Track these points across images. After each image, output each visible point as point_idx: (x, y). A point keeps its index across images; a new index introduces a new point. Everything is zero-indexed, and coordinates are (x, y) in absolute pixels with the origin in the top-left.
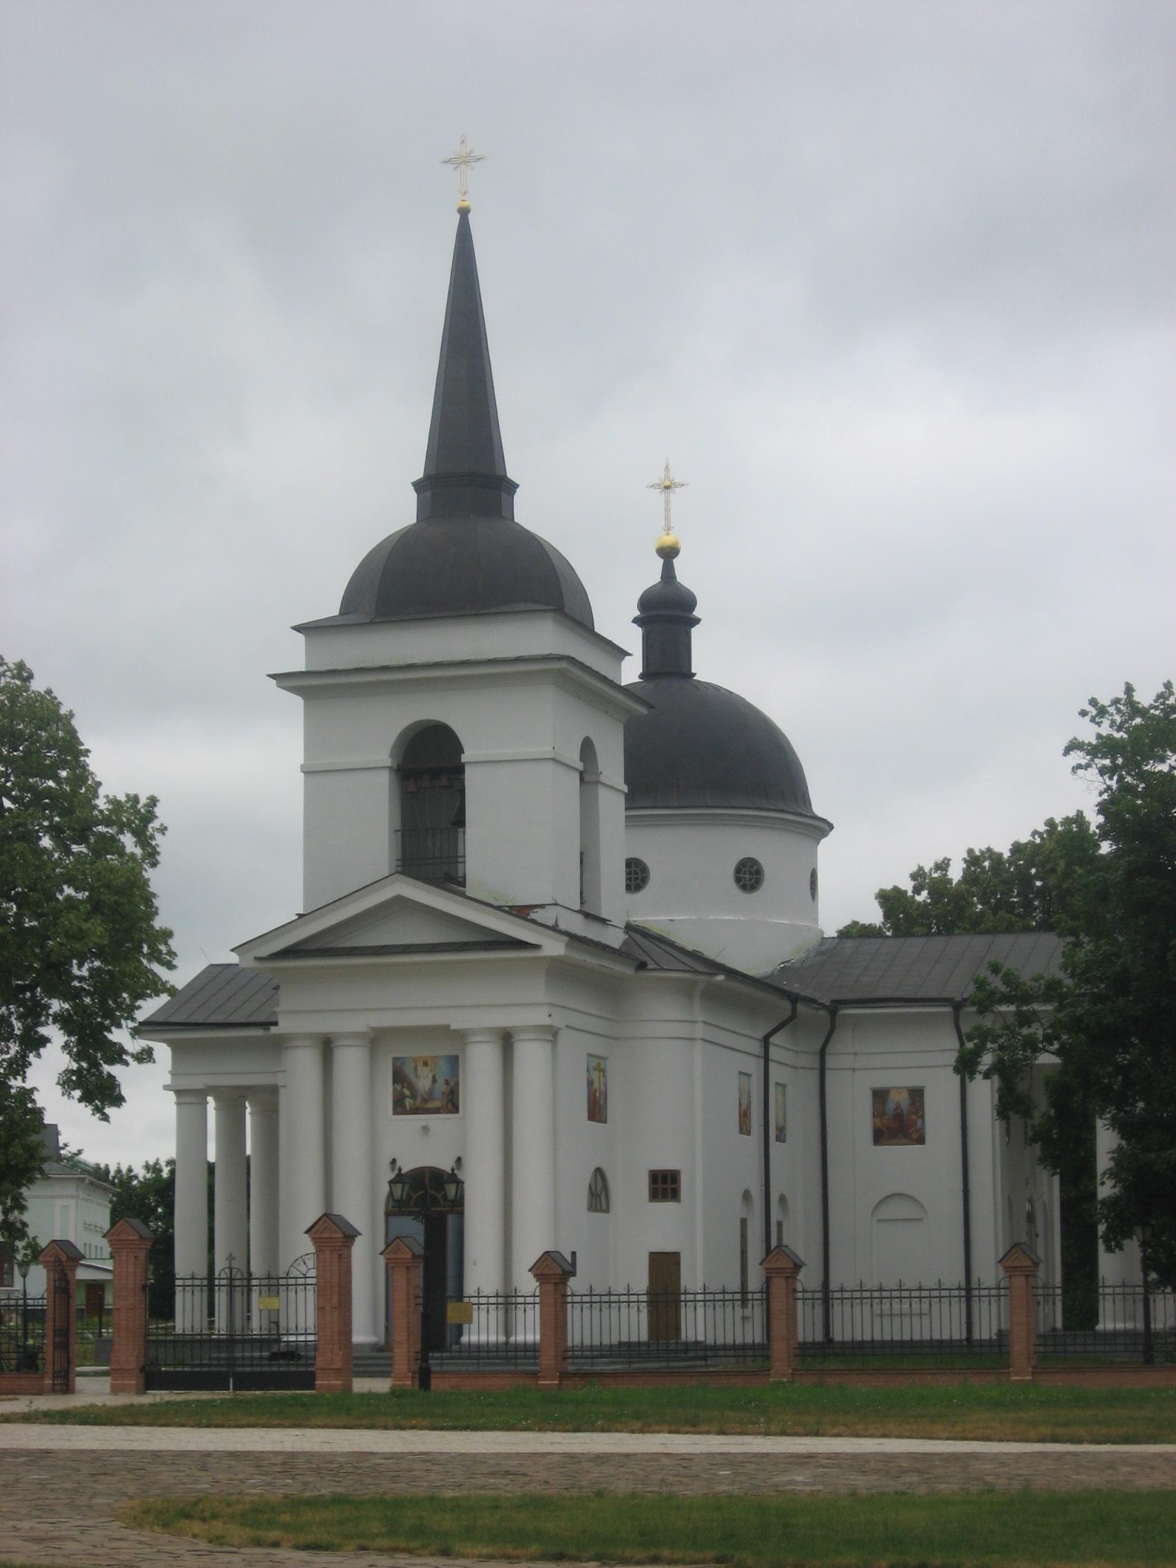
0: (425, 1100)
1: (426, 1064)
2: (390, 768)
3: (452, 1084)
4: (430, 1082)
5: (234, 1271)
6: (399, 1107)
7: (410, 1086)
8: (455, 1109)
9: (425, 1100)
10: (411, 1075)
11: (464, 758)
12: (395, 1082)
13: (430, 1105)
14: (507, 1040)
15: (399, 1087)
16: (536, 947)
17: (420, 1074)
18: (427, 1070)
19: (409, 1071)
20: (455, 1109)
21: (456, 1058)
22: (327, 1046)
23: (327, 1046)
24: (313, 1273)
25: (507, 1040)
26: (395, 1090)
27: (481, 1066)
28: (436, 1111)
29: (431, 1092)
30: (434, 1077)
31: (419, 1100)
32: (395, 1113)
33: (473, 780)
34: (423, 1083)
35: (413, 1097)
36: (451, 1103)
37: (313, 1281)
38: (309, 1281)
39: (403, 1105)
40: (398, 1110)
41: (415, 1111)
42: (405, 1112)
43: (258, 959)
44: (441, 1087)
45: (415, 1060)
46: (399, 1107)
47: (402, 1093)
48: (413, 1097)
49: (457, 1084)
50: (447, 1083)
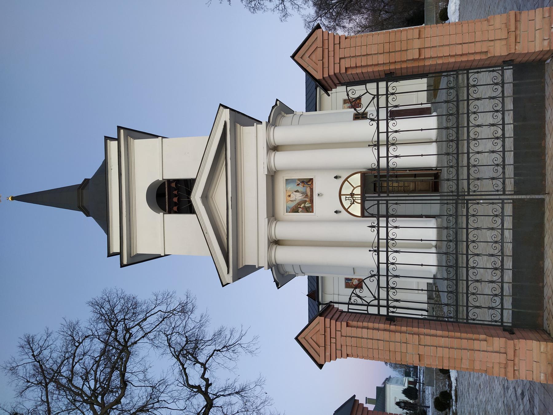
1: (289, 196)
2: (164, 214)
6: (309, 210)
7: (299, 204)
8: (311, 180)
9: (307, 195)
10: (294, 204)
11: (159, 178)
12: (298, 212)
13: (309, 194)
14: (274, 148)
15: (300, 210)
18: (292, 195)
19: (293, 204)
20: (311, 180)
22: (276, 242)
23: (276, 242)
25: (274, 148)
26: (302, 212)
28: (312, 190)
29: (303, 193)
30: (295, 192)
33: (170, 176)
34: (298, 197)
35: (305, 202)
36: (309, 182)
38: (382, 91)
39: (309, 207)
41: (312, 201)
43: (228, 273)
44: (301, 188)
45: (287, 202)
46: (309, 210)
47: (303, 208)
48: (305, 202)
49: (299, 180)
50: (298, 185)
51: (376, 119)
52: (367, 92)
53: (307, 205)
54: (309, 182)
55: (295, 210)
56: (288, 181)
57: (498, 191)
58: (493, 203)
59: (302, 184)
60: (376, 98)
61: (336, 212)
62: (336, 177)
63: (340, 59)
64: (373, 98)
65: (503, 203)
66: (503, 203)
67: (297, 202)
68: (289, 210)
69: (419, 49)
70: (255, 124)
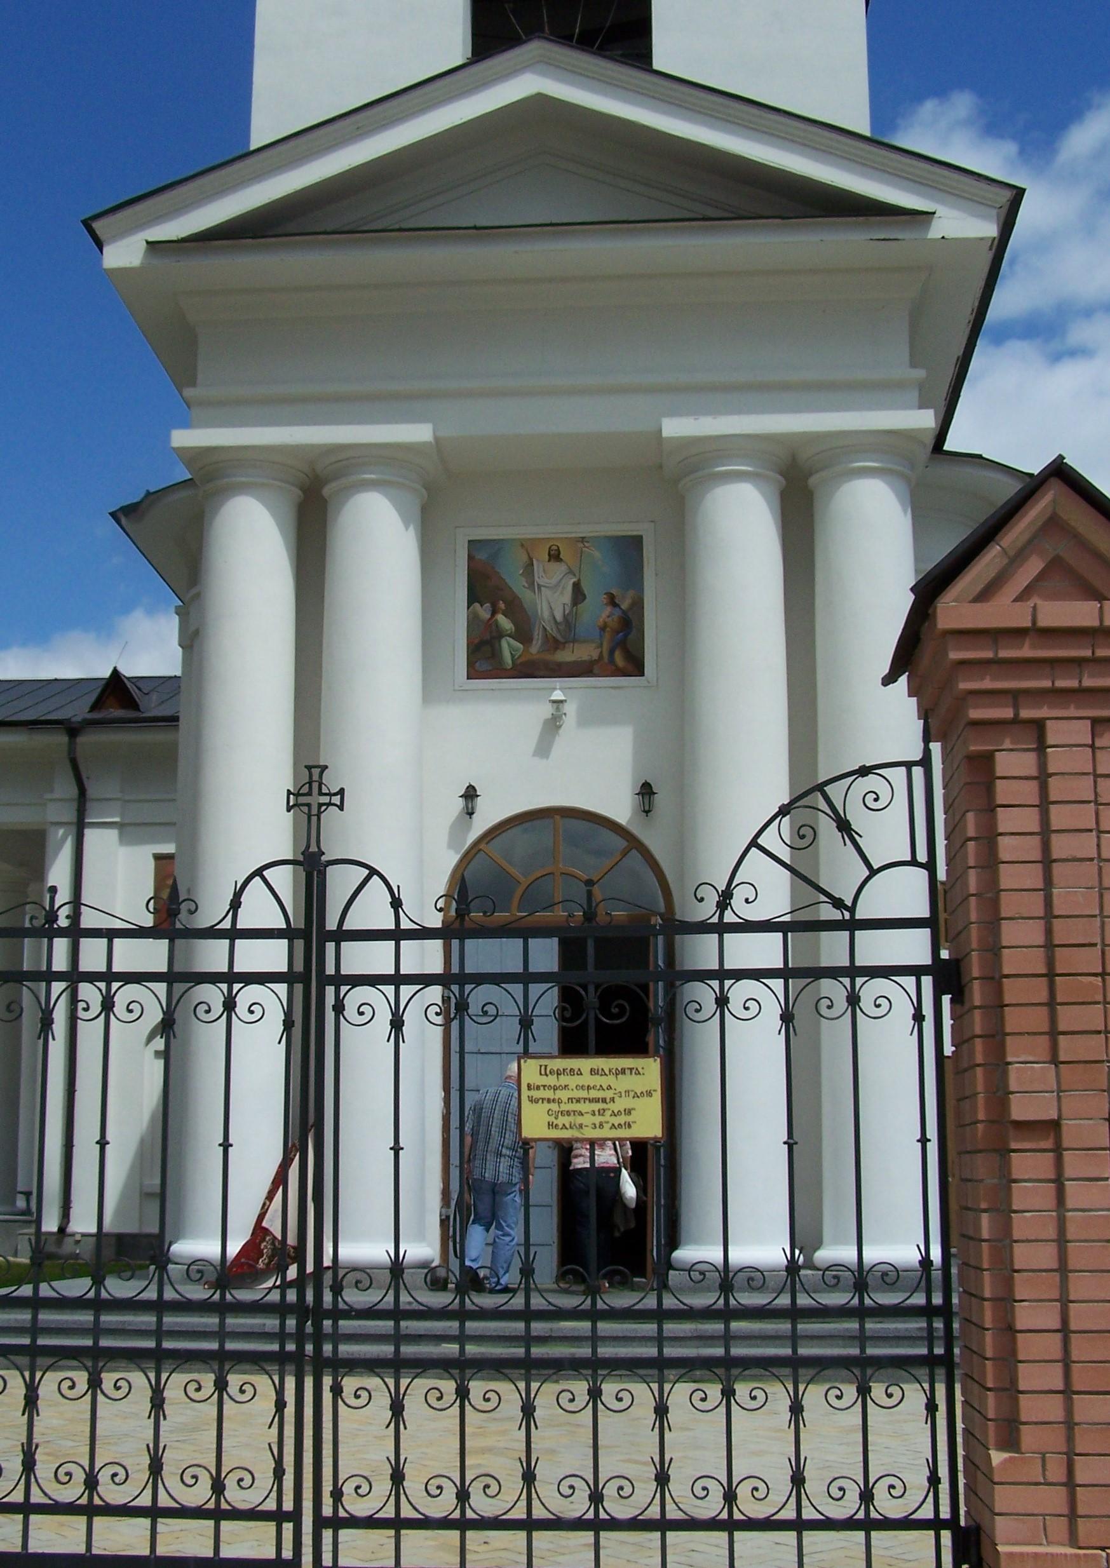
0: (554, 644)
1: (555, 556)
3: (624, 606)
4: (567, 597)
5: (340, 882)
6: (485, 659)
7: (515, 608)
8: (636, 667)
9: (554, 644)
10: (517, 584)
12: (472, 598)
13: (566, 656)
15: (484, 612)
16: (924, 217)
17: (539, 578)
18: (559, 569)
20: (636, 667)
21: (636, 542)
24: (906, 893)
26: (473, 621)
27: (741, 526)
29: (569, 623)
30: (577, 587)
31: (535, 648)
32: (473, 673)
34: (550, 600)
37: (914, 947)
38: (877, 948)
40: (481, 666)
41: (526, 670)
42: (498, 671)
44: (595, 612)
45: (524, 544)
46: (485, 659)
48: (523, 635)
49: (638, 605)
50: (612, 601)
51: (729, 917)
52: (873, 872)
53: (509, 648)
54: (623, 653)
55: (484, 585)
56: (629, 550)
57: (337, 1494)
58: (279, 1473)
59: (614, 622)
60: (836, 915)
61: (470, 794)
62: (646, 791)
63: (1039, 726)
64: (838, 903)
65: (278, 1516)
66: (278, 1516)
67: (526, 595)
68: (481, 556)
69: (1054, 1126)
70: (920, 374)
